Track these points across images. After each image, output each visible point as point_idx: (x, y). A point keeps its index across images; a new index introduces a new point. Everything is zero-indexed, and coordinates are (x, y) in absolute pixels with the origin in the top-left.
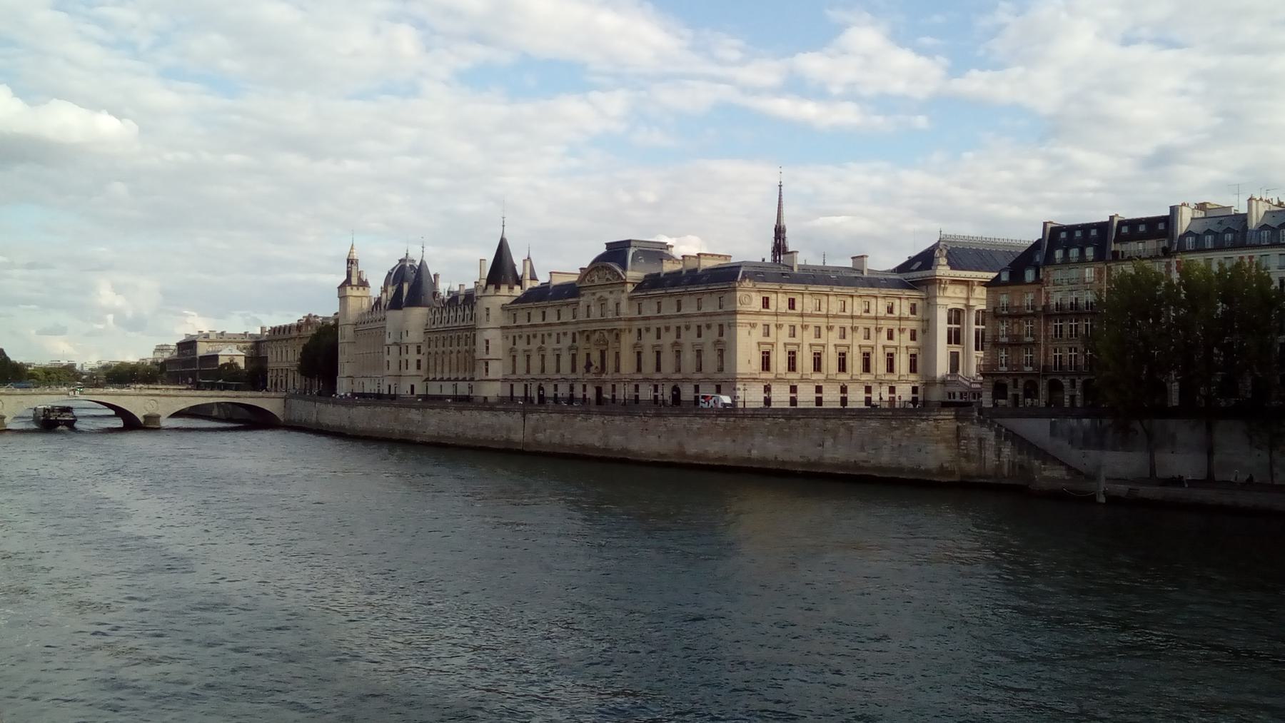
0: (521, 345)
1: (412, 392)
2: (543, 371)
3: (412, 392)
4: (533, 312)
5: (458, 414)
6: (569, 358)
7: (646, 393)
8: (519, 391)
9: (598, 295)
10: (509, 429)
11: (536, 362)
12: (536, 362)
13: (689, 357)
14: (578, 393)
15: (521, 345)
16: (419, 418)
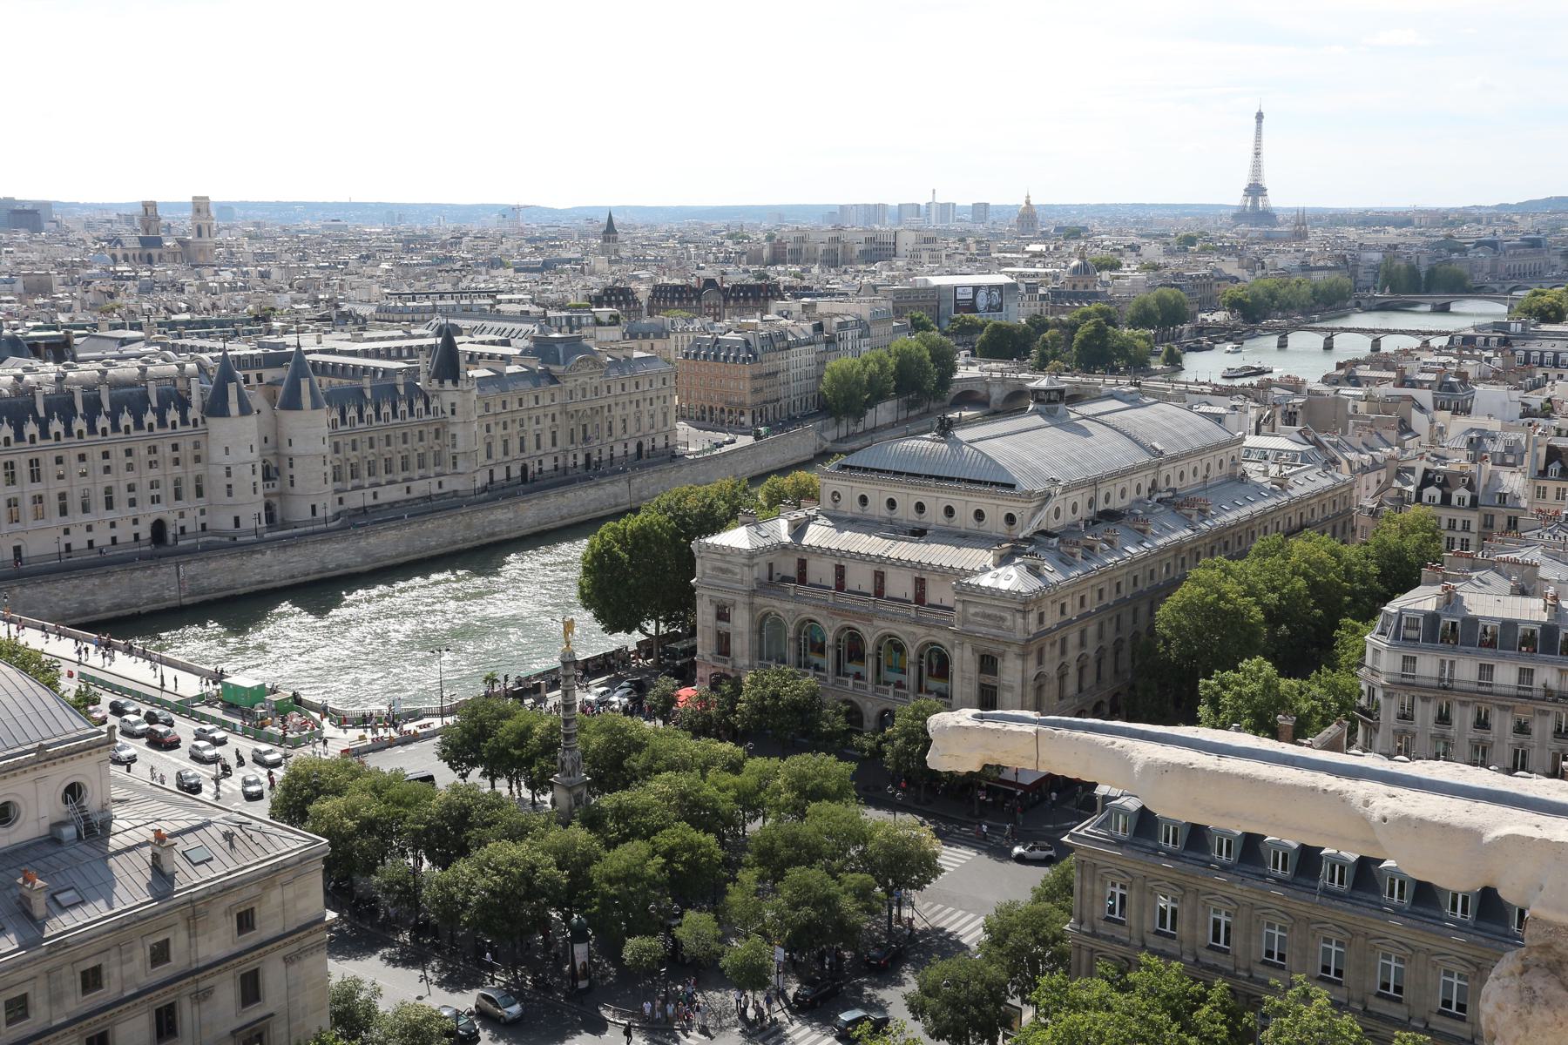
0: (498, 431)
1: (314, 513)
2: (522, 450)
3: (314, 513)
4: (509, 400)
5: (560, 499)
6: (549, 436)
7: (619, 450)
8: (500, 475)
9: (581, 380)
10: (616, 496)
11: (514, 445)
12: (514, 445)
13: (646, 420)
14: (560, 463)
15: (498, 431)
16: (511, 515)
